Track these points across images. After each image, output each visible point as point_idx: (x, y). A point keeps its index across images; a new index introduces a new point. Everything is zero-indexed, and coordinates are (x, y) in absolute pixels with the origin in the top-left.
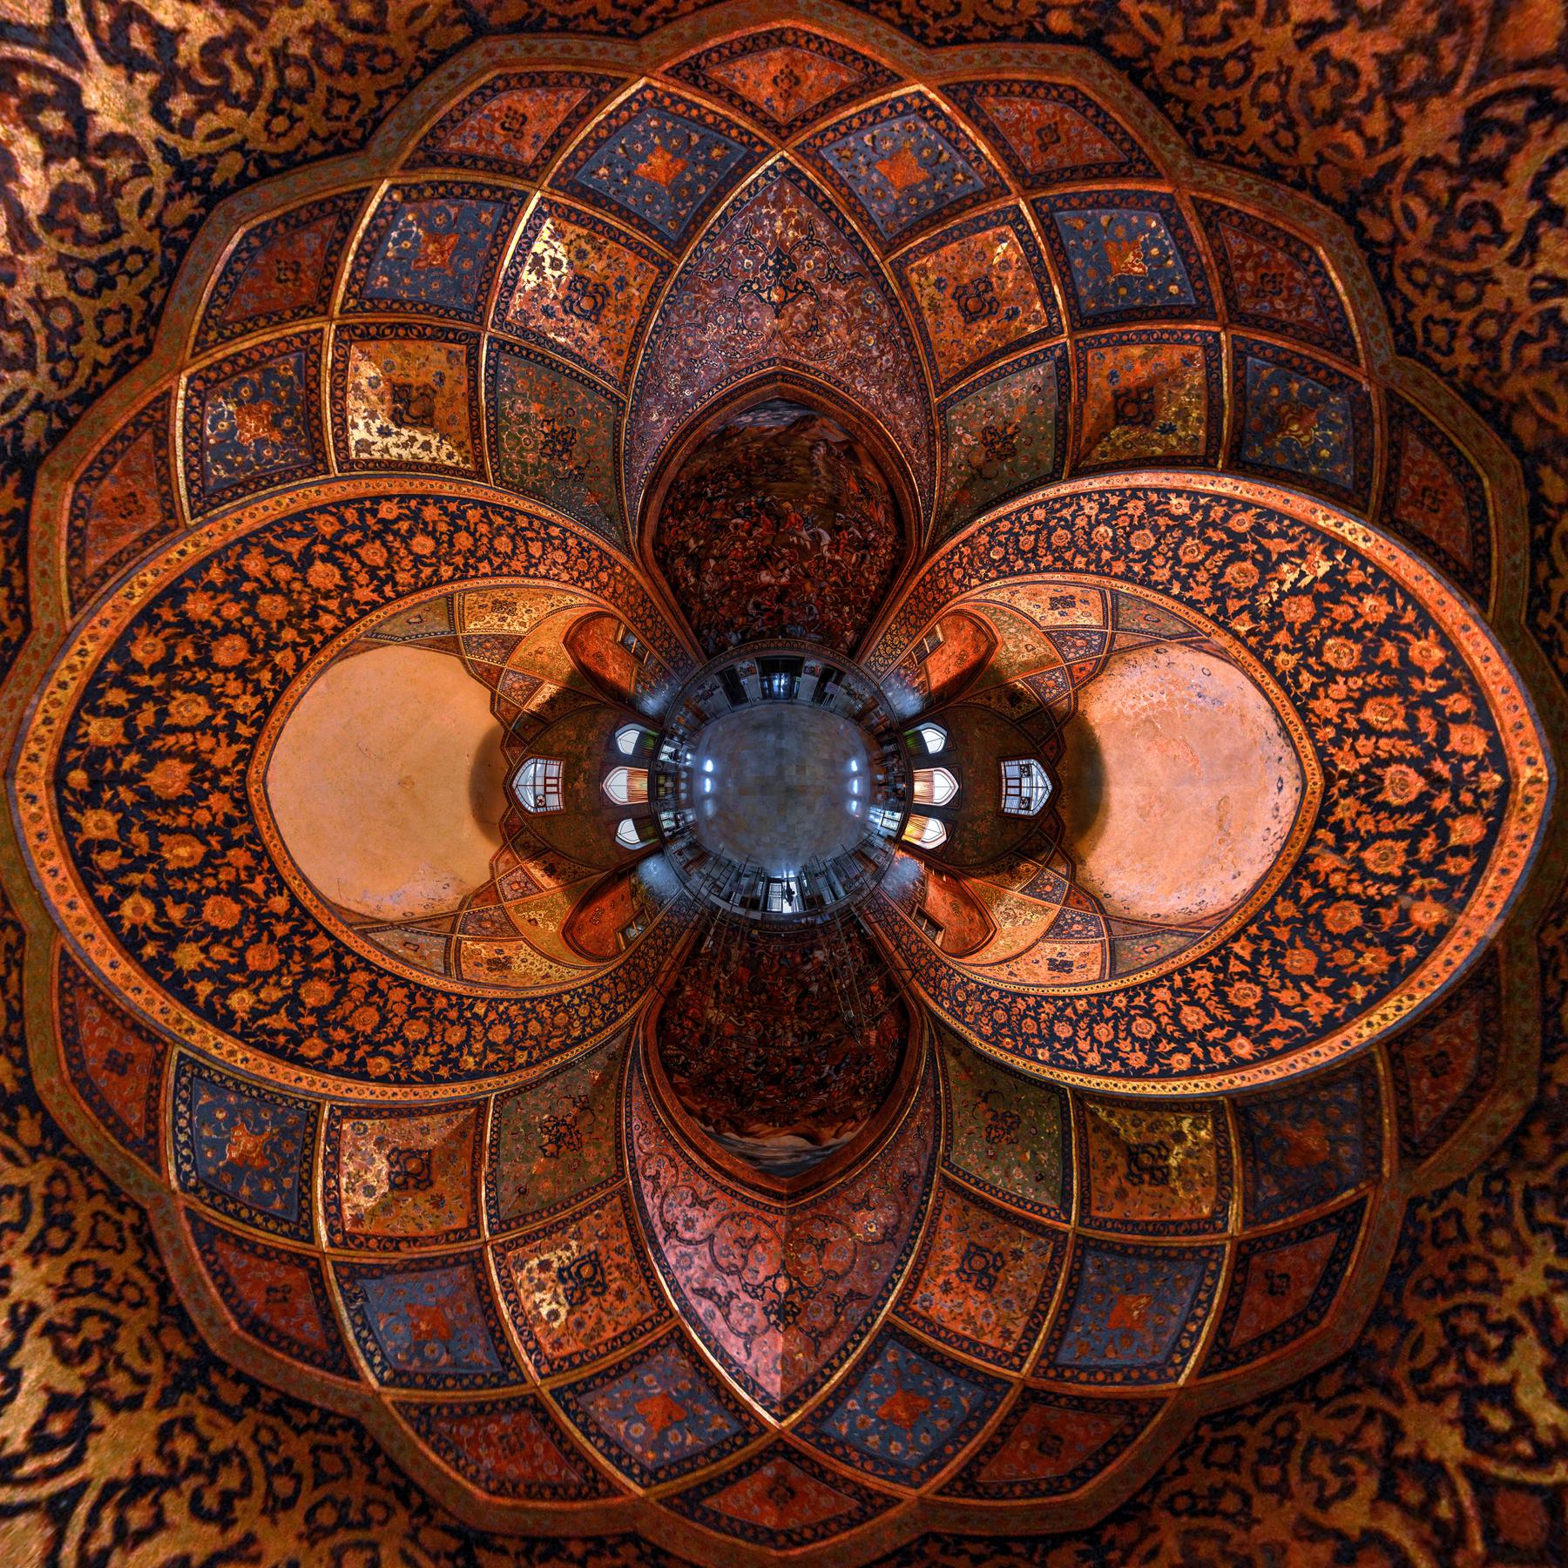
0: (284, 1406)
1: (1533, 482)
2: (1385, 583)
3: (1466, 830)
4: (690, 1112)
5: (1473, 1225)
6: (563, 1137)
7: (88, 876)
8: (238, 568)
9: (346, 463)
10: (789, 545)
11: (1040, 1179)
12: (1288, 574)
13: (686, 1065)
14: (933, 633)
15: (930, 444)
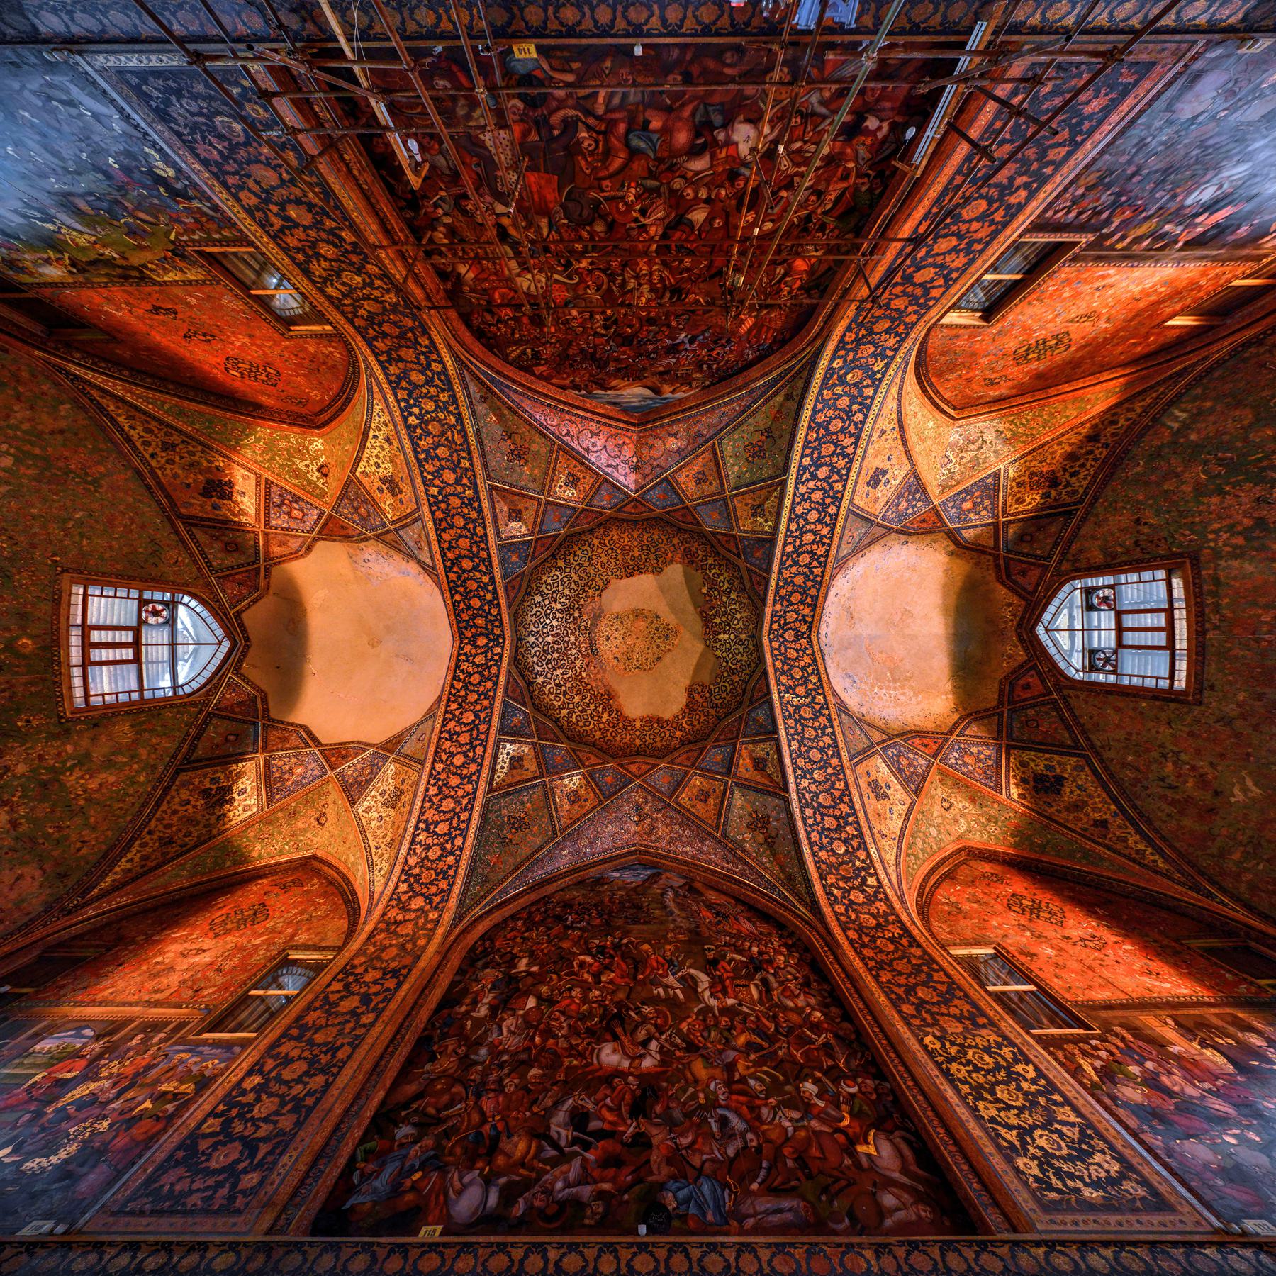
2: (779, 683)
3: (775, 626)
4: (563, 388)
6: (519, 454)
7: (501, 621)
9: (500, 741)
10: (654, 1000)
12: (795, 701)
13: (536, 355)
14: (971, 965)
15: (735, 855)
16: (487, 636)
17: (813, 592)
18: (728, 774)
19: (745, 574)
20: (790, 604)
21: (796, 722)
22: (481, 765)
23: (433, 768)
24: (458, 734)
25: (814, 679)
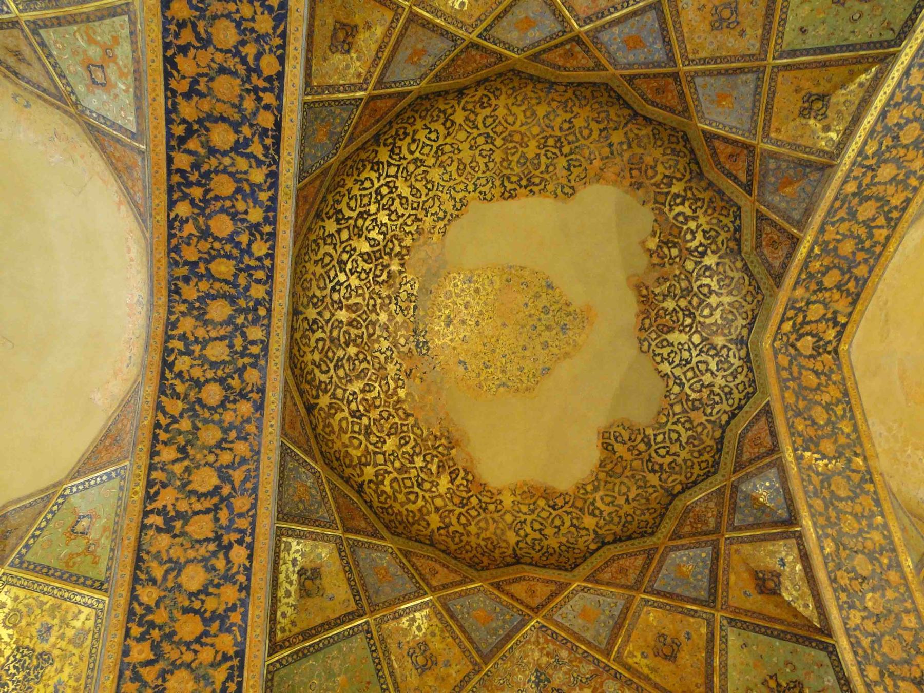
0: (398, 115)
1: (728, 423)
5: (722, 218)
8: (246, 439)
11: (803, 31)
16: (232, 300)
17: (861, 271)
18: (710, 601)
19: (749, 222)
20: (821, 288)
21: (828, 504)
22: (245, 588)
23: (134, 598)
24: (184, 517)
25: (846, 428)
